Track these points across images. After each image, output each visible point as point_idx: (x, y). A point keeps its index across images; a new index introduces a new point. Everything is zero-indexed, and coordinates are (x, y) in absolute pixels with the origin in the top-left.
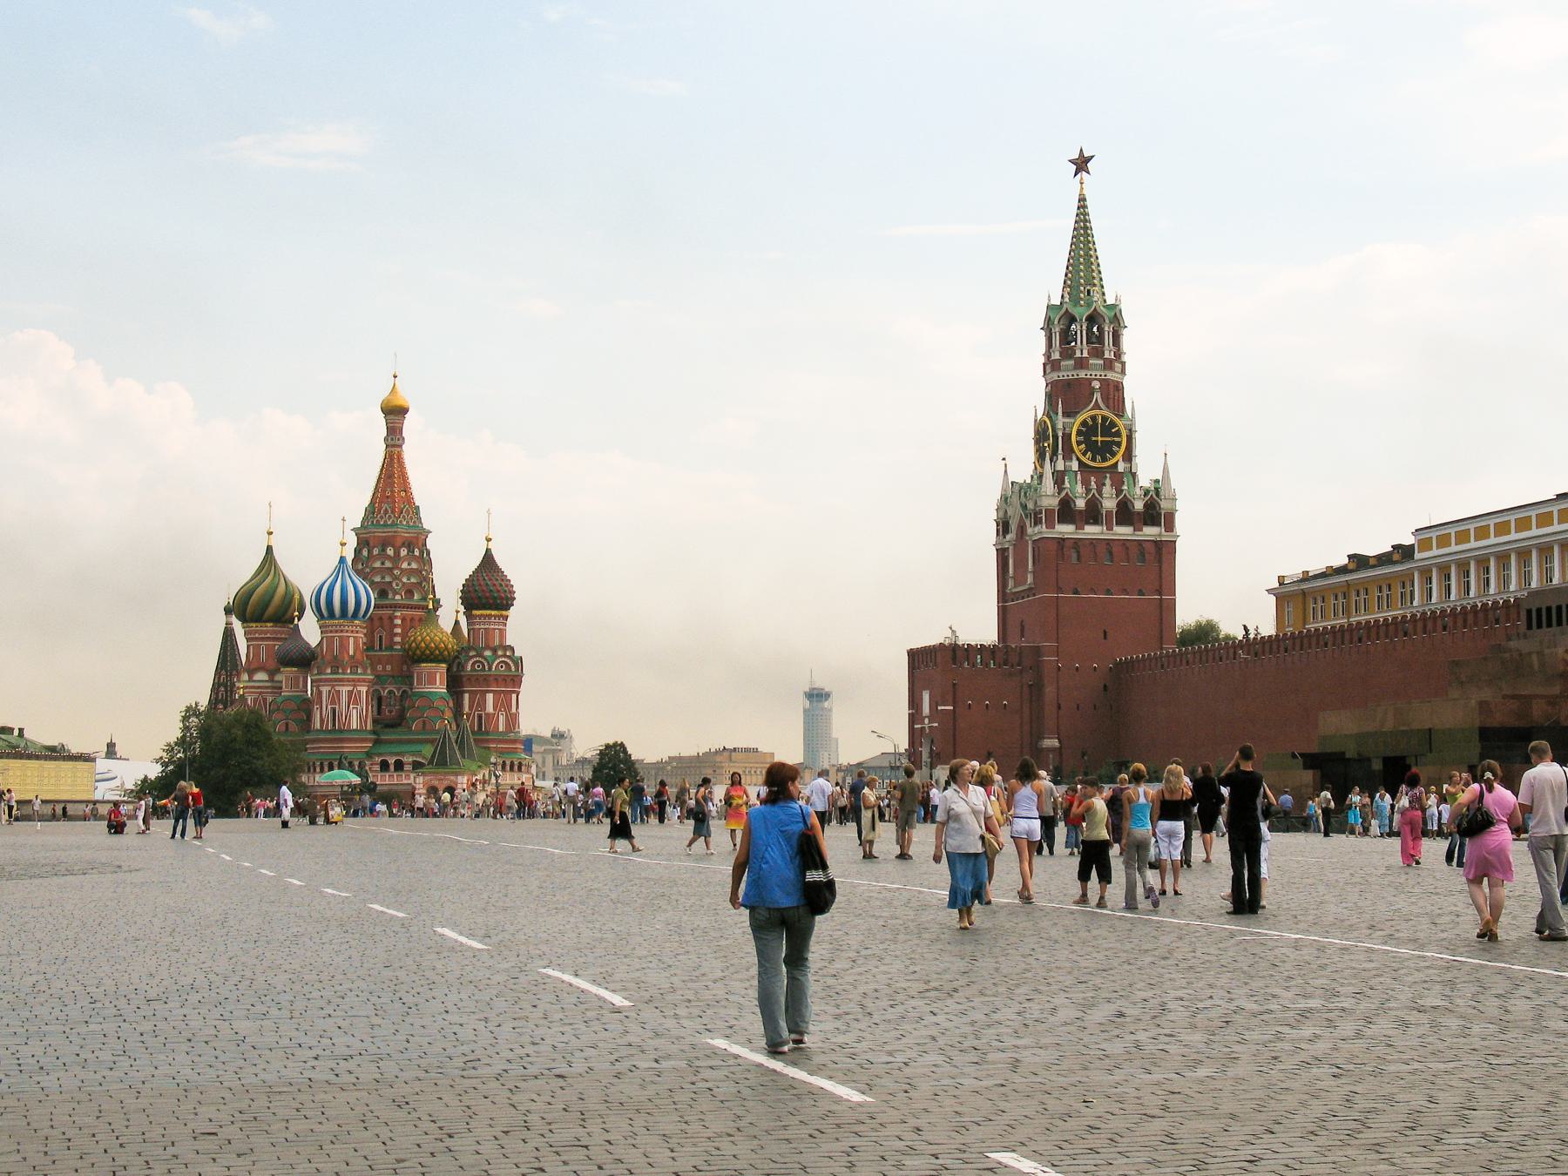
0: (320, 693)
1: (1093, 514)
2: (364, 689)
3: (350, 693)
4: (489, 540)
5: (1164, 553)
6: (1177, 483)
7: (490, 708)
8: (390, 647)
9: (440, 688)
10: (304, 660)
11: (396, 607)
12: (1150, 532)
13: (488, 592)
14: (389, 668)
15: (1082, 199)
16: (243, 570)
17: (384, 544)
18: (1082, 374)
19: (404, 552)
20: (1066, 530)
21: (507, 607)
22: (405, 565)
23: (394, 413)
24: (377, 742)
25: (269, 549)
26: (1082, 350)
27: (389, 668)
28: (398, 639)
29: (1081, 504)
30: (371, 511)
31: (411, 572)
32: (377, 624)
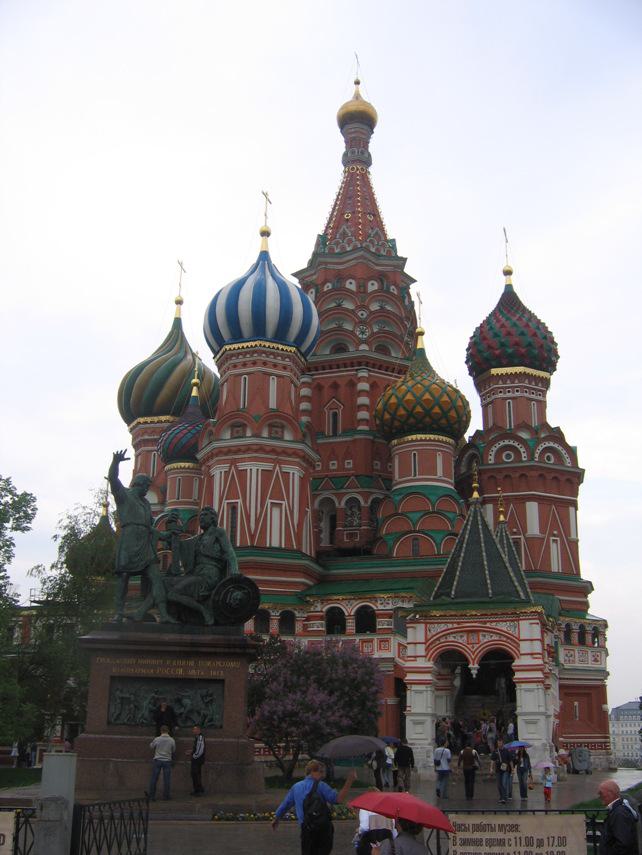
0: (211, 478)
2: (295, 472)
3: (267, 474)
4: (508, 273)
7: (533, 527)
8: (350, 429)
9: (441, 479)
13: (514, 345)
14: (349, 464)
17: (340, 277)
22: (375, 307)
23: (357, 123)
24: (322, 581)
25: (178, 323)
27: (349, 464)
28: (363, 415)
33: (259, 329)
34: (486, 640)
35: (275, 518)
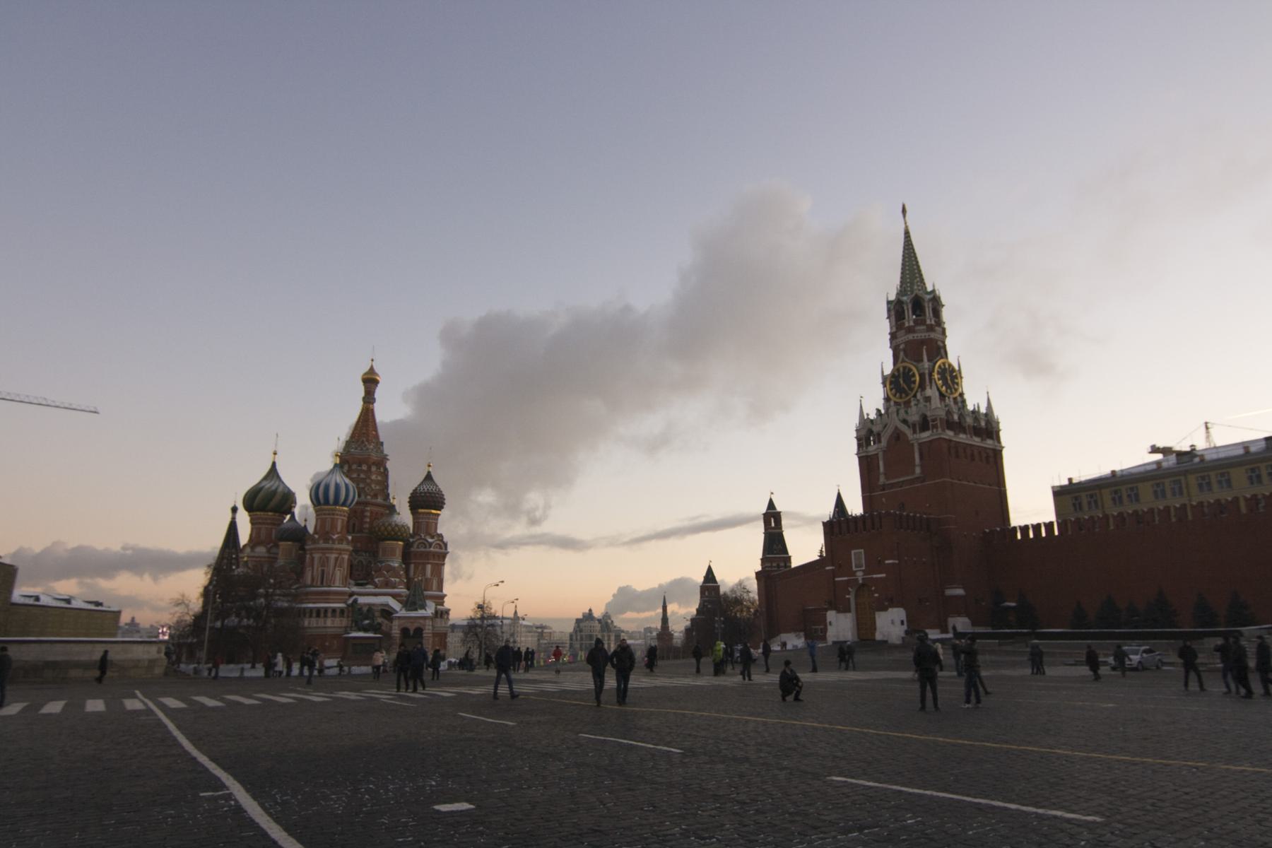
0: (313, 559)
1: (958, 427)
2: (346, 557)
3: (337, 559)
5: (995, 457)
6: (998, 412)
10: (298, 535)
11: (367, 504)
12: (989, 443)
15: (907, 234)
16: (254, 476)
18: (933, 335)
19: (374, 469)
20: (950, 434)
21: (440, 507)
22: (373, 477)
23: (370, 381)
25: (274, 464)
26: (930, 320)
29: (956, 417)
30: (348, 444)
31: (378, 483)
32: (356, 516)
33: (336, 502)
34: (416, 625)
35: (338, 574)
